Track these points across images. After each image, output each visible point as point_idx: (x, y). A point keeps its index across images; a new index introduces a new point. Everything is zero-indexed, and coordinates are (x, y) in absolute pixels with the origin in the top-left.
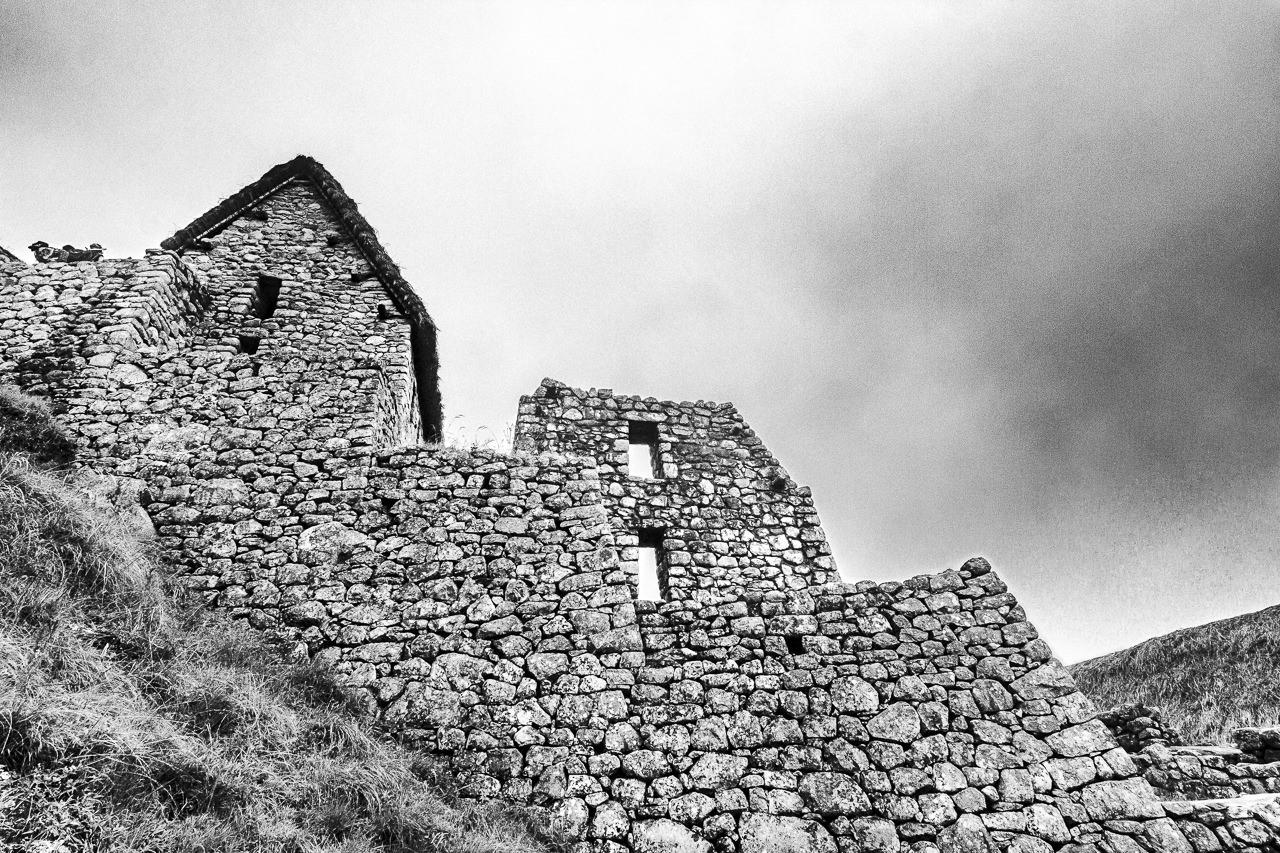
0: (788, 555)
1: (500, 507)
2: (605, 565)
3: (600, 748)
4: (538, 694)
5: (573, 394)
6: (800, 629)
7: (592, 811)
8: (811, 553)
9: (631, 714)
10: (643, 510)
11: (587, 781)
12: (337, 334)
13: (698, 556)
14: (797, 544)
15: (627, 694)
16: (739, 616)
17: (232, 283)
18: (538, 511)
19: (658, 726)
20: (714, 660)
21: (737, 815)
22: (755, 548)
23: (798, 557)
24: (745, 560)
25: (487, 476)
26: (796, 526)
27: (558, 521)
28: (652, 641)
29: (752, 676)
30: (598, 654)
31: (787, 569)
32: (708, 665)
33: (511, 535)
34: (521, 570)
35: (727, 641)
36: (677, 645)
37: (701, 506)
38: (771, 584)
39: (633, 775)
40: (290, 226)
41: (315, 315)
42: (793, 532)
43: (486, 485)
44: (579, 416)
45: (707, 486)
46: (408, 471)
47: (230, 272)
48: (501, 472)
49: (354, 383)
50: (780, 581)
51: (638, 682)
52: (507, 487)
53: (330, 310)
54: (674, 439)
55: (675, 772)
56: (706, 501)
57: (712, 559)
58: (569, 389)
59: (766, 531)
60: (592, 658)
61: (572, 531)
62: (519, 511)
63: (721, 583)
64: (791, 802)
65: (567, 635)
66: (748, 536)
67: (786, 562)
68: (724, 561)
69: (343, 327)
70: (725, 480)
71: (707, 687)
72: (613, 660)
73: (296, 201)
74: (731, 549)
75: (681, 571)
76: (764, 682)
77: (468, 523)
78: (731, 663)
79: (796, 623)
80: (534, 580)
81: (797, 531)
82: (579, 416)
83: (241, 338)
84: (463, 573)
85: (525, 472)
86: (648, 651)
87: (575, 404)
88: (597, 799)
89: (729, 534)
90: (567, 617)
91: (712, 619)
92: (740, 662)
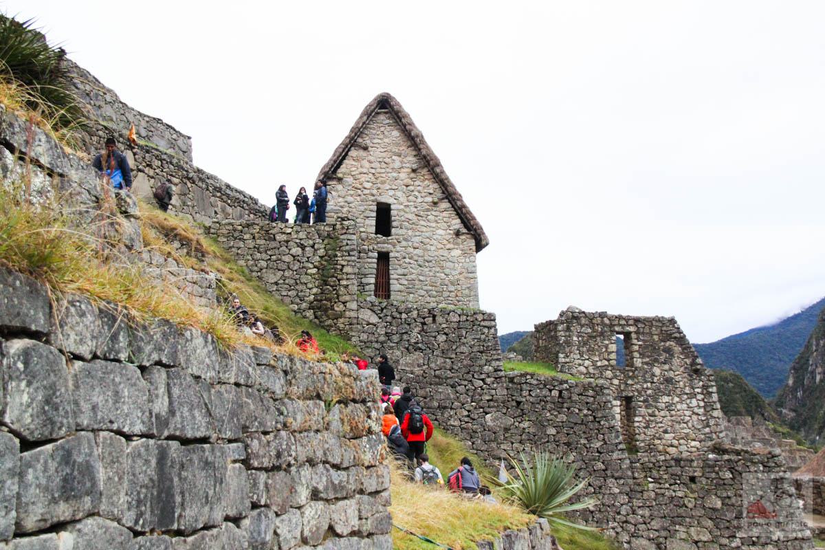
0: (696, 410)
1: (569, 409)
2: (617, 441)
3: (619, 513)
4: (594, 493)
5: (586, 316)
6: (696, 474)
7: (617, 533)
8: (708, 409)
9: (629, 502)
10: (623, 387)
11: (616, 524)
12: (433, 248)
13: (650, 411)
14: (702, 404)
15: (627, 494)
16: (671, 467)
17: (362, 208)
18: (585, 412)
19: (639, 507)
20: (660, 484)
21: (666, 538)
22: (679, 406)
23: (701, 411)
24: (673, 412)
25: (560, 392)
26: (702, 393)
27: (595, 418)
28: (636, 475)
29: (674, 491)
30: (616, 479)
31: (695, 417)
32: (658, 486)
33: (576, 424)
34: (583, 441)
35: (665, 476)
36: (646, 477)
37: (652, 383)
38: (685, 425)
39: (630, 523)
40: (384, 155)
41: (417, 233)
42: (700, 397)
43: (560, 396)
44: (589, 330)
45: (657, 371)
46: (524, 386)
47: (358, 198)
48: (567, 390)
49: (486, 330)
50: (690, 425)
51: (631, 491)
52: (570, 398)
53: (424, 229)
54: (640, 343)
55: (645, 523)
56: (655, 381)
57: (657, 413)
58: (584, 312)
59: (685, 397)
60: (614, 480)
61: (602, 423)
62: (577, 411)
63: (660, 425)
64: (684, 536)
65: (604, 470)
66: (676, 399)
67: (694, 413)
68: (662, 413)
69: (435, 243)
70: (666, 367)
71: (657, 494)
72: (622, 481)
73: (382, 129)
74: (666, 407)
75: (641, 419)
76: (680, 494)
77: (556, 416)
78: (667, 485)
79: (695, 471)
80: (588, 446)
81: (702, 396)
82: (589, 330)
83: (379, 253)
84: (558, 441)
85: (577, 390)
86: (634, 478)
87: (587, 322)
88: (619, 530)
89: (666, 399)
90: (603, 463)
91: (660, 467)
92: (670, 485)
